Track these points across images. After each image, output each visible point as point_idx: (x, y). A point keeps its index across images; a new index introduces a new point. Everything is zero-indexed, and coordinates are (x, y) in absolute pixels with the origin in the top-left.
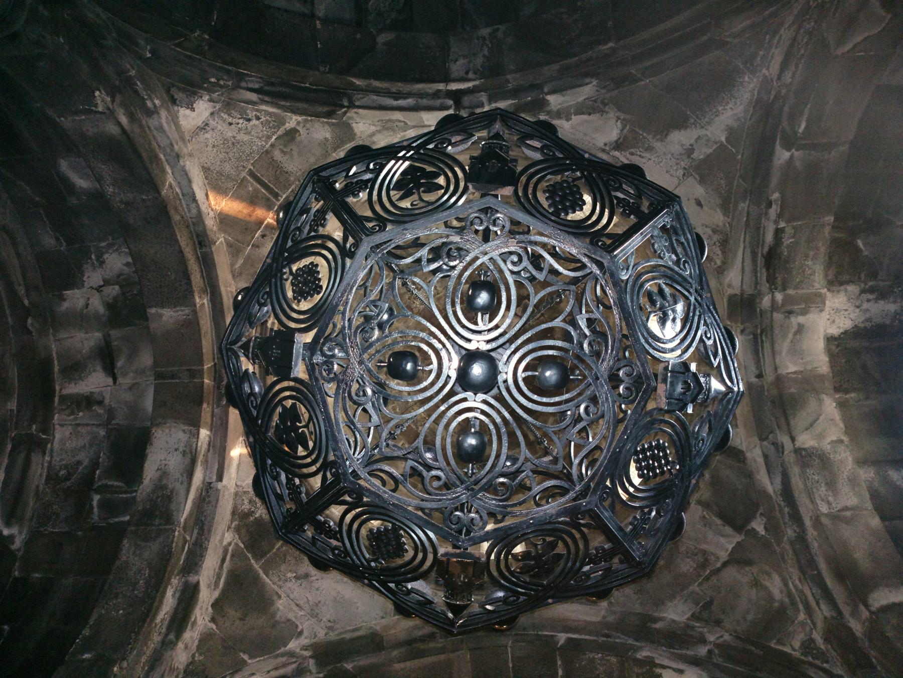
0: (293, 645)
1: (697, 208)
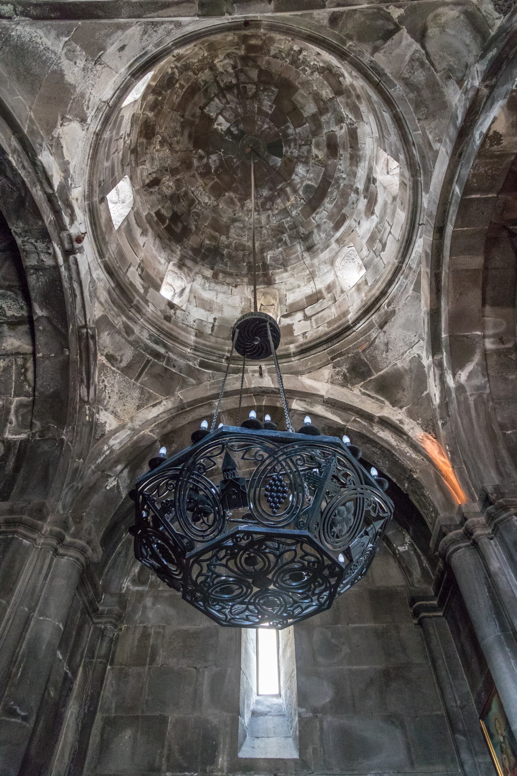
1: (127, 48)
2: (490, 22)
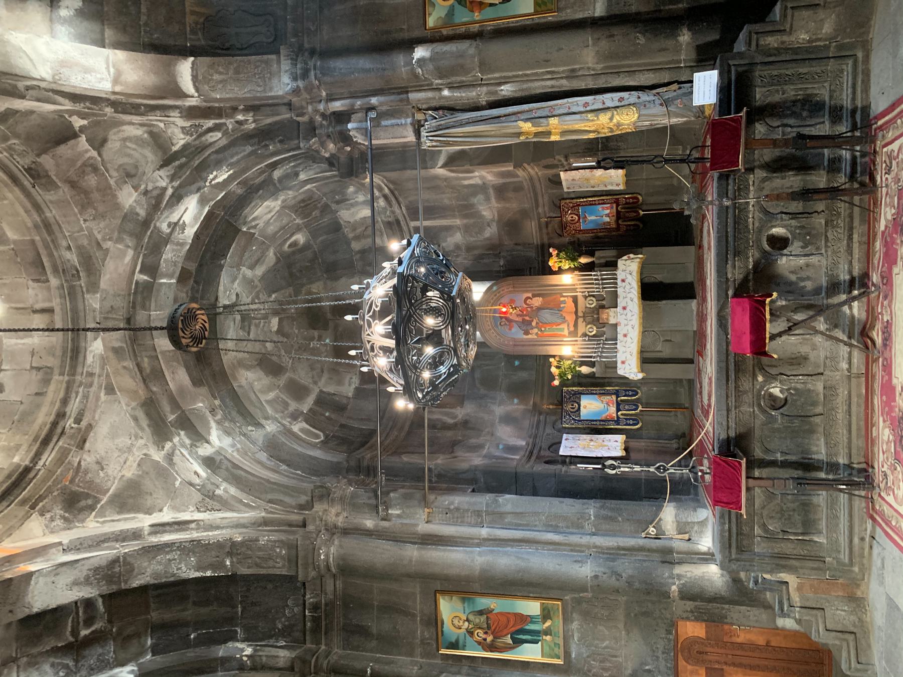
0: (158, 456)
2: (174, 141)
